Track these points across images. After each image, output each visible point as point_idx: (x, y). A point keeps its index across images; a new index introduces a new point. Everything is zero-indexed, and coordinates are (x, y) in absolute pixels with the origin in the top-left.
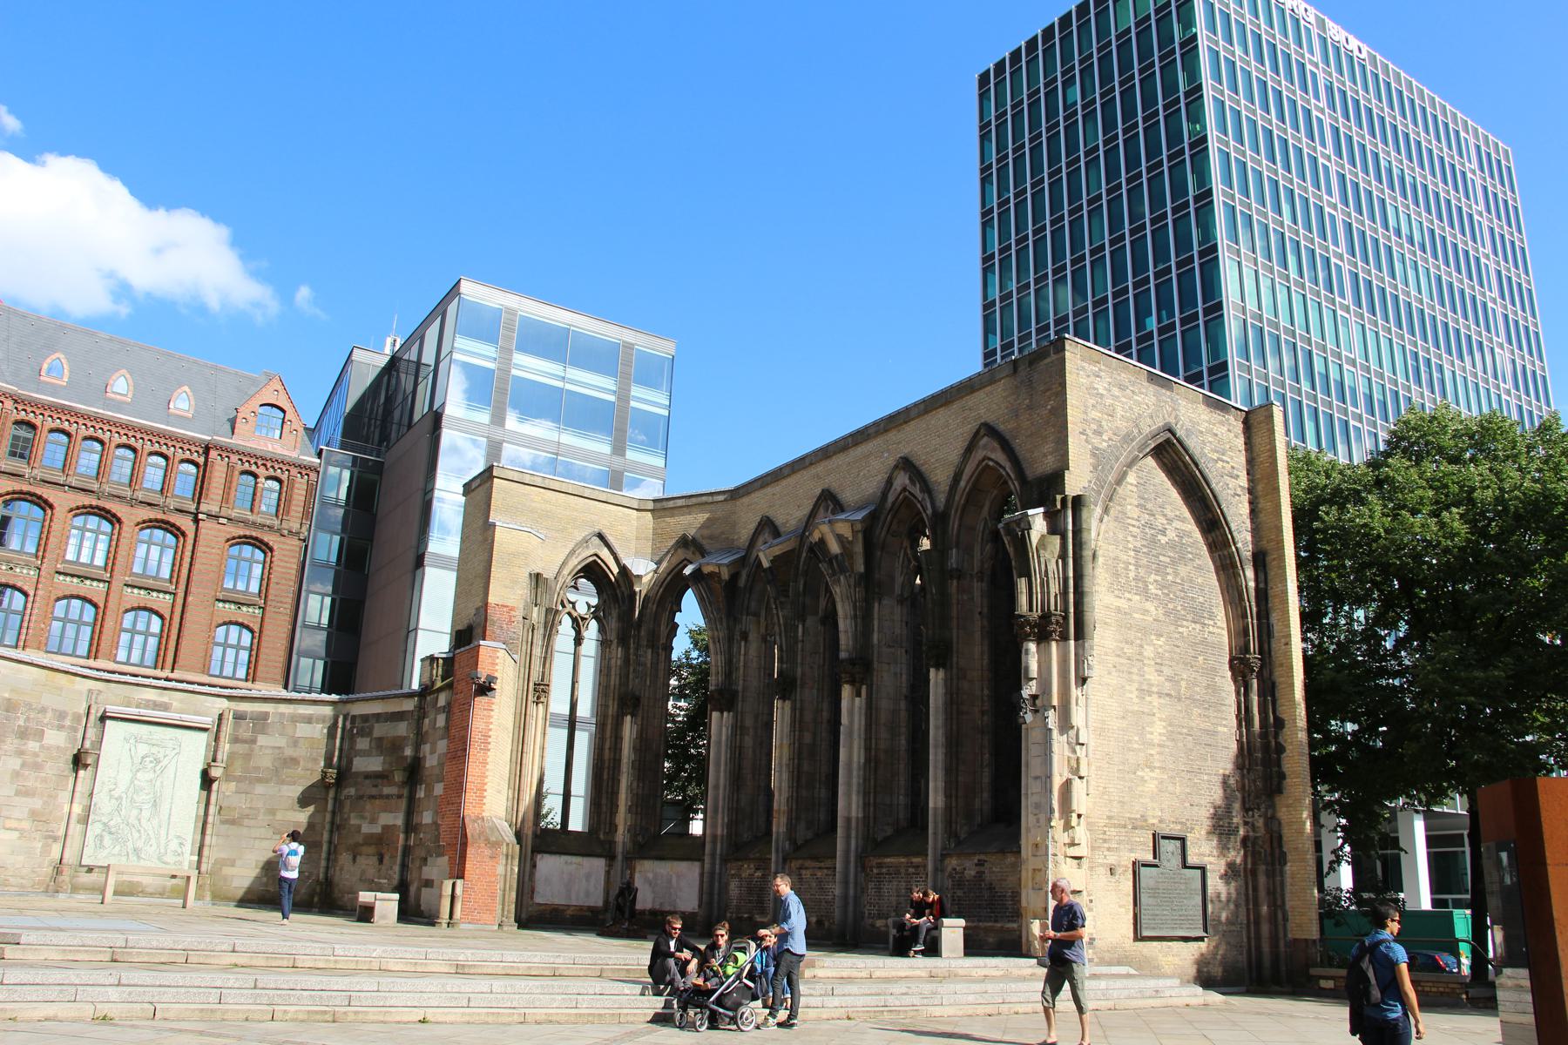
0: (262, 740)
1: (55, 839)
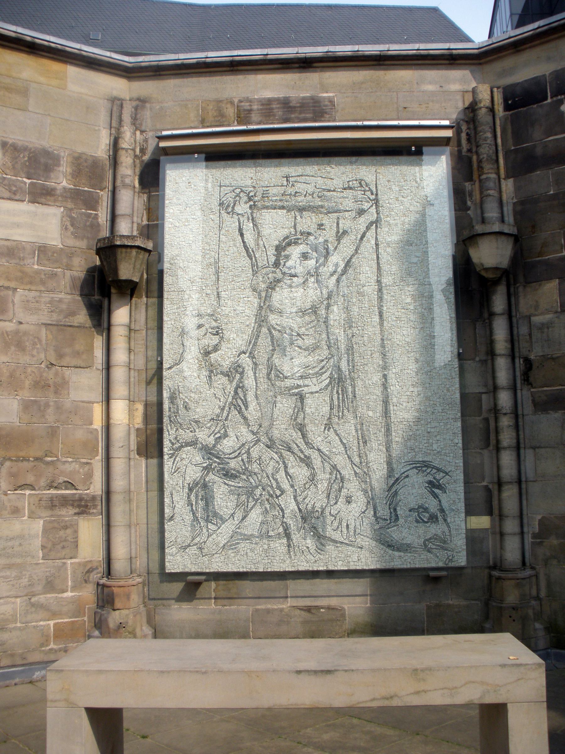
1: (83, 506)
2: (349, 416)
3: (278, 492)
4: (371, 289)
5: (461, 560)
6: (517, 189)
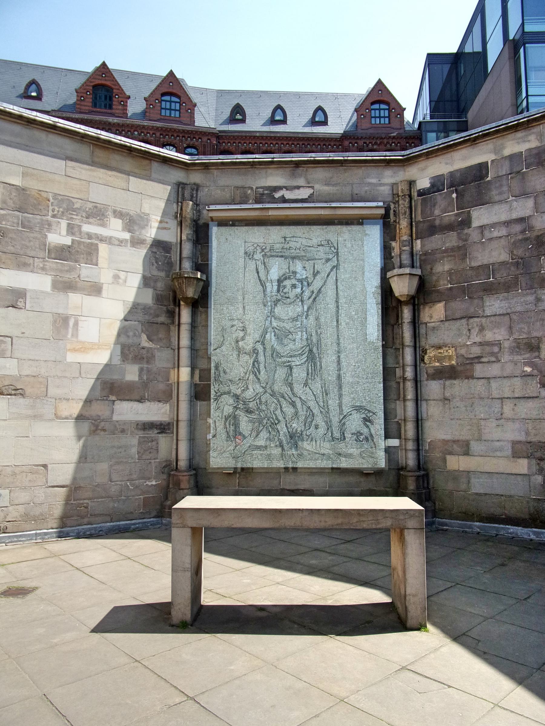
0: (480, 216)
2: (318, 379)
3: (276, 422)
4: (332, 306)
5: (382, 464)
6: (423, 246)
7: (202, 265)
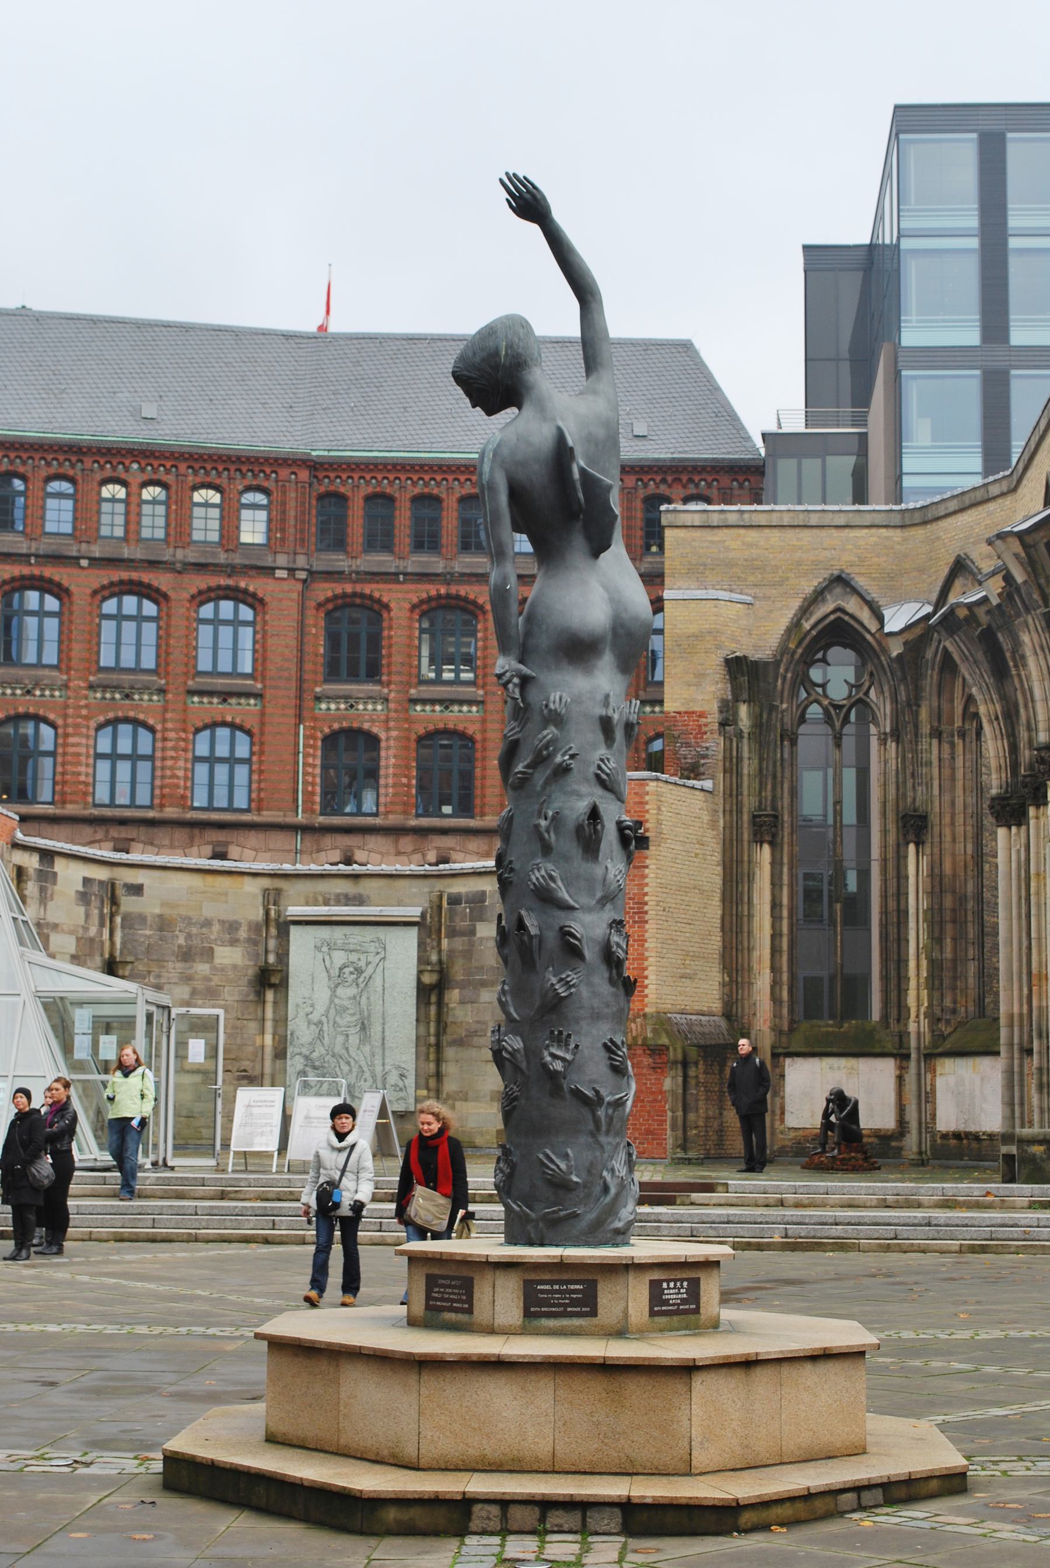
4: (380, 989)
6: (449, 944)
7: (283, 956)
